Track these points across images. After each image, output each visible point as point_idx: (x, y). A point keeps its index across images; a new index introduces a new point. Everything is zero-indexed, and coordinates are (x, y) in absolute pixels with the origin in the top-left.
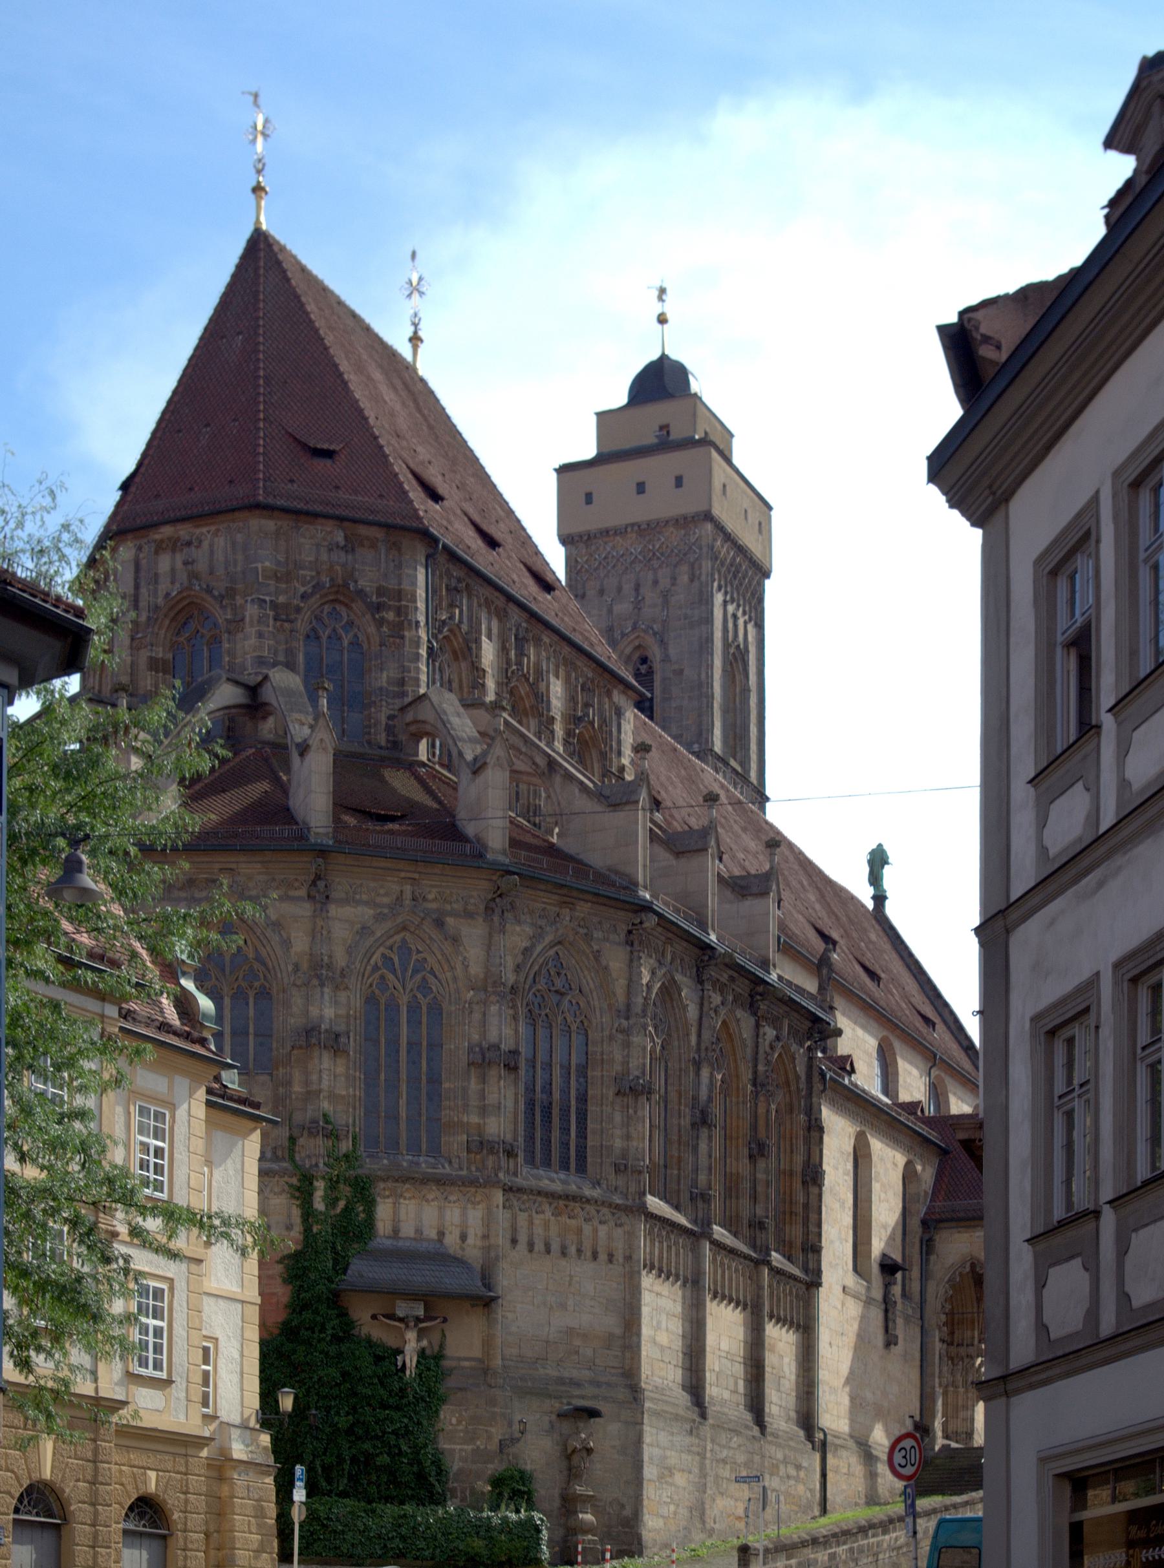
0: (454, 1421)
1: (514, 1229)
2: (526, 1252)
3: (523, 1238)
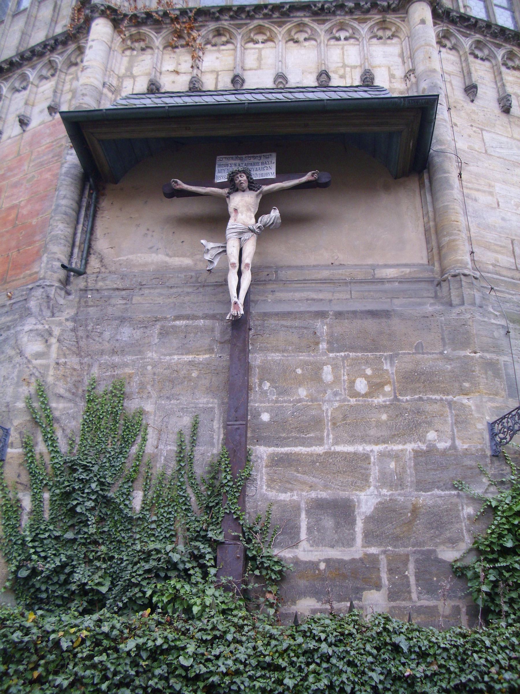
0: (361, 385)
1: (466, 73)
2: (495, 109)
3: (488, 93)
